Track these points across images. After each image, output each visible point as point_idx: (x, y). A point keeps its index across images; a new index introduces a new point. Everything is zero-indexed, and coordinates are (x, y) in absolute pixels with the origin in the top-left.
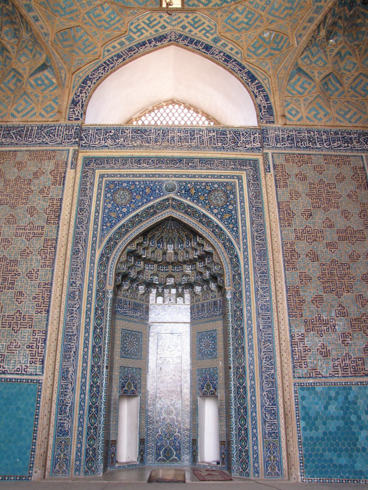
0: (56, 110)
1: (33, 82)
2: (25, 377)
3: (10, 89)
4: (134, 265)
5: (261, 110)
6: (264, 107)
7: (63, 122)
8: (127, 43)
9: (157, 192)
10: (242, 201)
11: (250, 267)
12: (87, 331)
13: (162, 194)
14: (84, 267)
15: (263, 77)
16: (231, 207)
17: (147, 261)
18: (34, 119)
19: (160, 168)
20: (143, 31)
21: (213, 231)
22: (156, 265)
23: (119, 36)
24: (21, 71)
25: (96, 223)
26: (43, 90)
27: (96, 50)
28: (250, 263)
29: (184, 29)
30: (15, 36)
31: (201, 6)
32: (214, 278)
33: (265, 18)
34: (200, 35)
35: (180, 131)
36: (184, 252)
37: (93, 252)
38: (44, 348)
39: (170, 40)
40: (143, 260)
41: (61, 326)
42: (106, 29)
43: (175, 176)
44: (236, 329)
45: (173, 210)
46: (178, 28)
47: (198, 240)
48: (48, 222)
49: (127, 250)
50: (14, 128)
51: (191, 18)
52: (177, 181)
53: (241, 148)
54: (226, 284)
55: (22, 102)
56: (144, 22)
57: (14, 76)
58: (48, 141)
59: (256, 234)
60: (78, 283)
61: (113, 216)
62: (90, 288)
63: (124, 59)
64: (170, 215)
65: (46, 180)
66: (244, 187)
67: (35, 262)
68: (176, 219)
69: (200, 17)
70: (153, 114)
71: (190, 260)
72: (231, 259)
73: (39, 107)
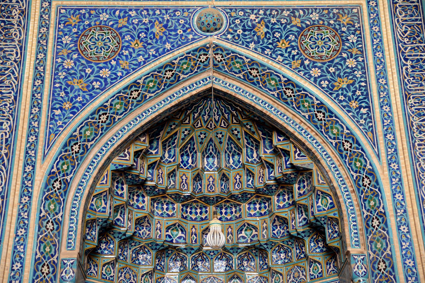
4: (128, 204)
9: (180, 32)
10: (378, 48)
11: (408, 199)
13: (190, 37)
16: (351, 63)
17: (159, 195)
21: (310, 119)
22: (178, 206)
25: (35, 103)
28: (406, 190)
32: (316, 229)
36: (243, 173)
37: (29, 169)
40: (148, 194)
45: (216, 75)
47: (275, 142)
49: (111, 167)
52: (224, 8)
54: (348, 241)
59: (416, 121)
61: (77, 86)
64: (209, 86)
66: (382, 15)
68: (225, 94)
71: (258, 191)
72: (357, 181)
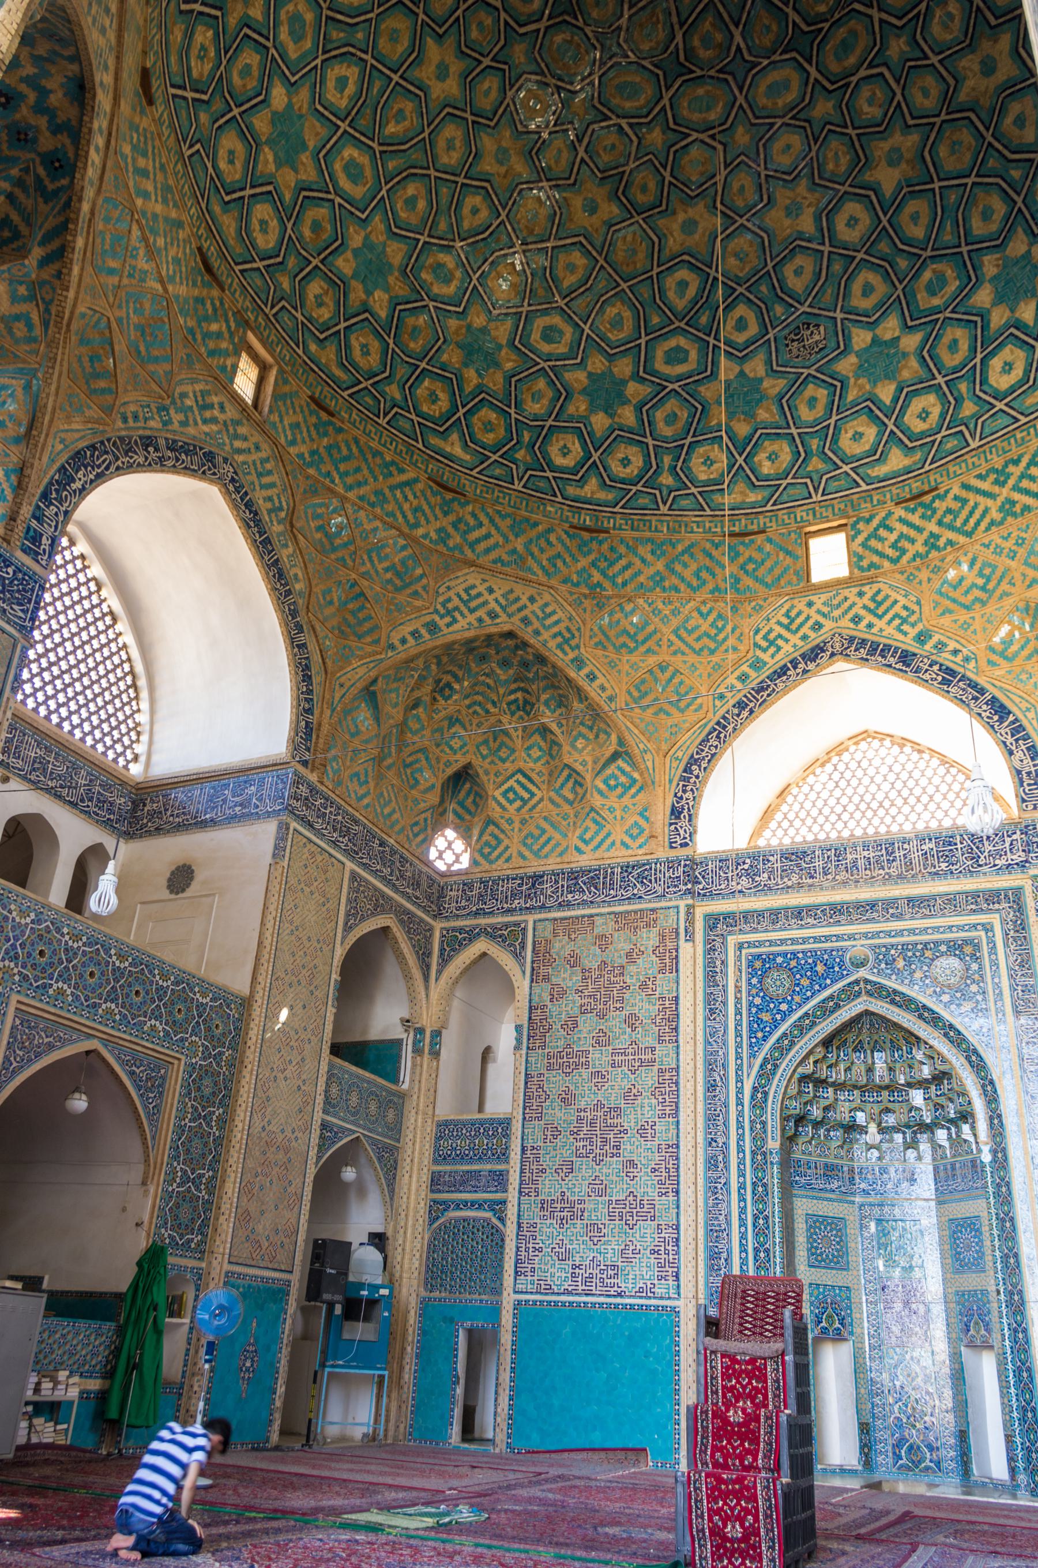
0: (647, 833)
1: (602, 786)
2: (653, 1302)
3: (566, 800)
5: (1021, 782)
6: (1029, 773)
7: (663, 853)
8: (753, 674)
12: (742, 1223)
14: (727, 1112)
15: (1024, 705)
17: (839, 1086)
18: (613, 853)
19: (838, 923)
20: (780, 642)
23: (737, 664)
24: (579, 768)
26: (621, 796)
27: (699, 701)
29: (856, 623)
30: (560, 704)
31: (886, 564)
33: (1018, 576)
34: (890, 630)
35: (866, 848)
38: (677, 1253)
39: (833, 655)
41: (701, 1215)
42: (712, 652)
43: (865, 936)
44: (1003, 1220)
46: (845, 622)
48: (660, 1041)
50: (584, 872)
51: (869, 595)
53: (985, 869)
55: (589, 823)
56: (779, 623)
57: (569, 776)
58: (641, 893)
60: (720, 1141)
62: (741, 1149)
63: (751, 712)
65: (647, 964)
67: (648, 1109)
69: (886, 590)
70: (829, 768)
73: (618, 828)
